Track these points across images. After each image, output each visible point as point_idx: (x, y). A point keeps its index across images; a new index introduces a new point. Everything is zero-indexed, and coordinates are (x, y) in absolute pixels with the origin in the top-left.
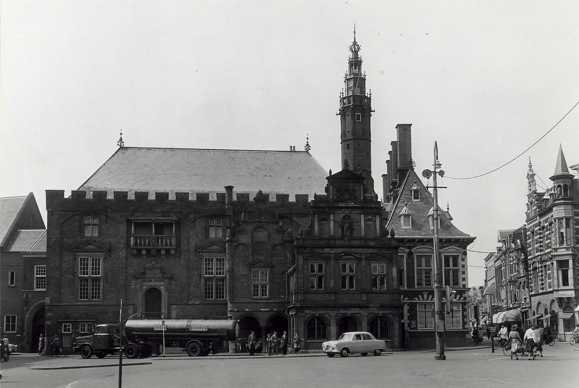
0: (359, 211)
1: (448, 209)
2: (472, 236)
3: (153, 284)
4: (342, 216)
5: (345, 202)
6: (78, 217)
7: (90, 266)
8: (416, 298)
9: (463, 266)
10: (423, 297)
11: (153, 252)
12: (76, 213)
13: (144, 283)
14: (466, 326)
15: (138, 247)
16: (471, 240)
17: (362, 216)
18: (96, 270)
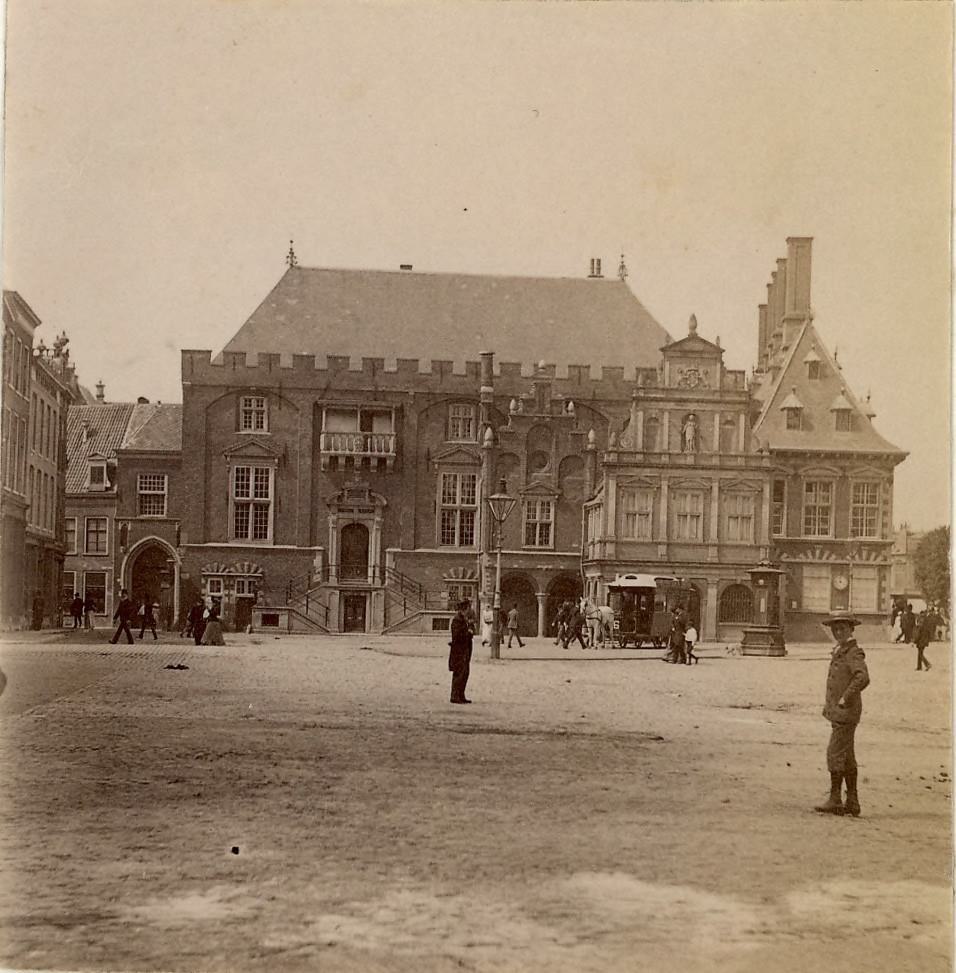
0: (709, 407)
1: (869, 398)
2: (904, 450)
3: (356, 516)
4: (685, 413)
5: (692, 391)
6: (234, 396)
7: (252, 483)
8: (801, 555)
9: (886, 502)
10: (814, 554)
11: (358, 463)
12: (231, 390)
13: (341, 515)
14: (883, 607)
15: (333, 452)
16: (900, 457)
17: (717, 418)
18: (262, 490)
